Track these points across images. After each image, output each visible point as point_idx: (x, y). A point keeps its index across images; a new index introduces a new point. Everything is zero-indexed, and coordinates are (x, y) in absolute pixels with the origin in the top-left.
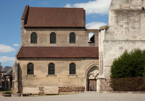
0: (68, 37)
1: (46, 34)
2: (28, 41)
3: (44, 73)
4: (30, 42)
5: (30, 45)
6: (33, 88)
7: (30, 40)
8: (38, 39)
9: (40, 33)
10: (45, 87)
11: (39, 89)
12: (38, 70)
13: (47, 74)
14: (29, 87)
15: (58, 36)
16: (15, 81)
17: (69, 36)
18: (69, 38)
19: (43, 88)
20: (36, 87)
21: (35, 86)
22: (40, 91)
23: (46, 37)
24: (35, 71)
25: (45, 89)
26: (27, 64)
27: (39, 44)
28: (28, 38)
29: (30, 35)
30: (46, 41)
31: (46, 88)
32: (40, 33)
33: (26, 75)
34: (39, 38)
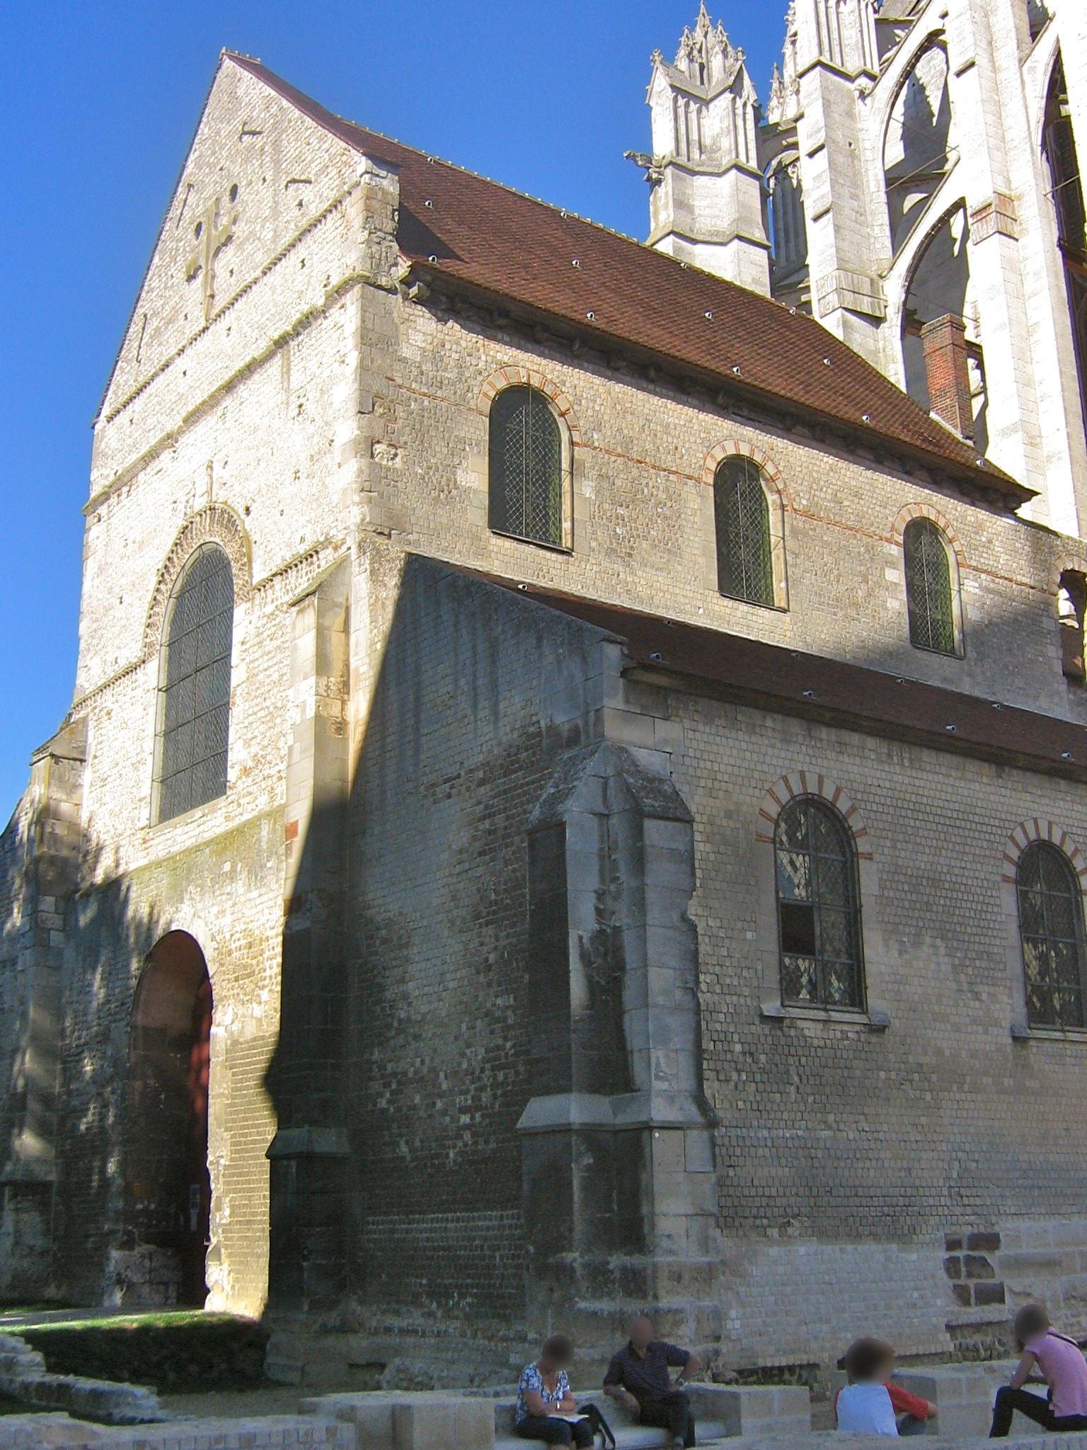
0: (893, 565)
1: (668, 461)
2: (448, 490)
3: (984, 990)
4: (478, 514)
5: (482, 552)
6: (872, 1253)
7: (474, 476)
8: (580, 498)
9: (598, 427)
10: (1023, 1233)
11: (952, 1267)
12: (917, 944)
13: (1009, 1006)
14: (822, 1234)
15: (800, 523)
16: (671, 1100)
17: (896, 552)
18: (896, 576)
19: (991, 1241)
20: (913, 1230)
21: (892, 1221)
22: (962, 1295)
23: (674, 497)
24: (878, 954)
25: (1019, 1264)
26: (773, 809)
27: (591, 569)
28: (457, 449)
29: (486, 406)
30: (672, 550)
31: (1025, 1250)
32: (598, 427)
33: (771, 1007)
34: (587, 489)
